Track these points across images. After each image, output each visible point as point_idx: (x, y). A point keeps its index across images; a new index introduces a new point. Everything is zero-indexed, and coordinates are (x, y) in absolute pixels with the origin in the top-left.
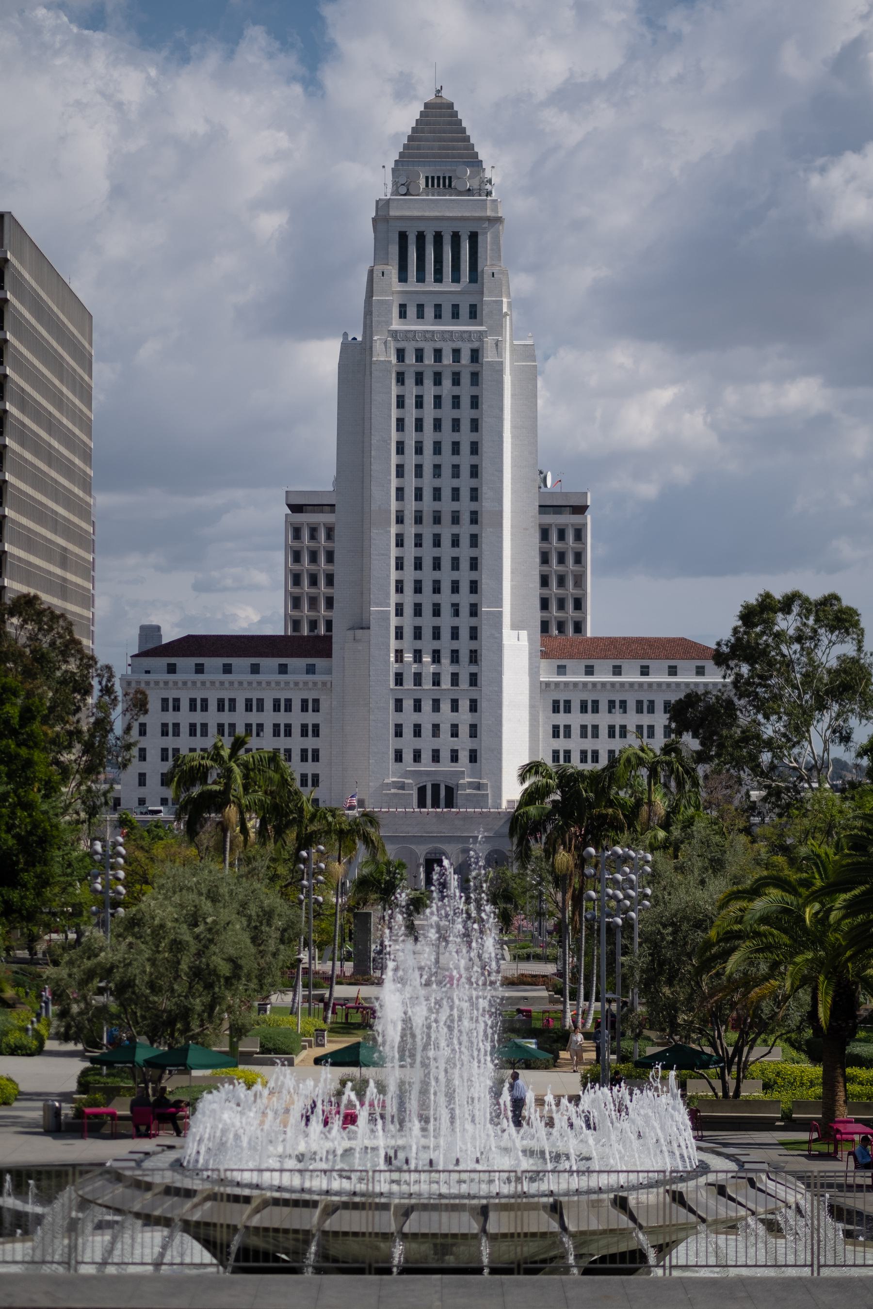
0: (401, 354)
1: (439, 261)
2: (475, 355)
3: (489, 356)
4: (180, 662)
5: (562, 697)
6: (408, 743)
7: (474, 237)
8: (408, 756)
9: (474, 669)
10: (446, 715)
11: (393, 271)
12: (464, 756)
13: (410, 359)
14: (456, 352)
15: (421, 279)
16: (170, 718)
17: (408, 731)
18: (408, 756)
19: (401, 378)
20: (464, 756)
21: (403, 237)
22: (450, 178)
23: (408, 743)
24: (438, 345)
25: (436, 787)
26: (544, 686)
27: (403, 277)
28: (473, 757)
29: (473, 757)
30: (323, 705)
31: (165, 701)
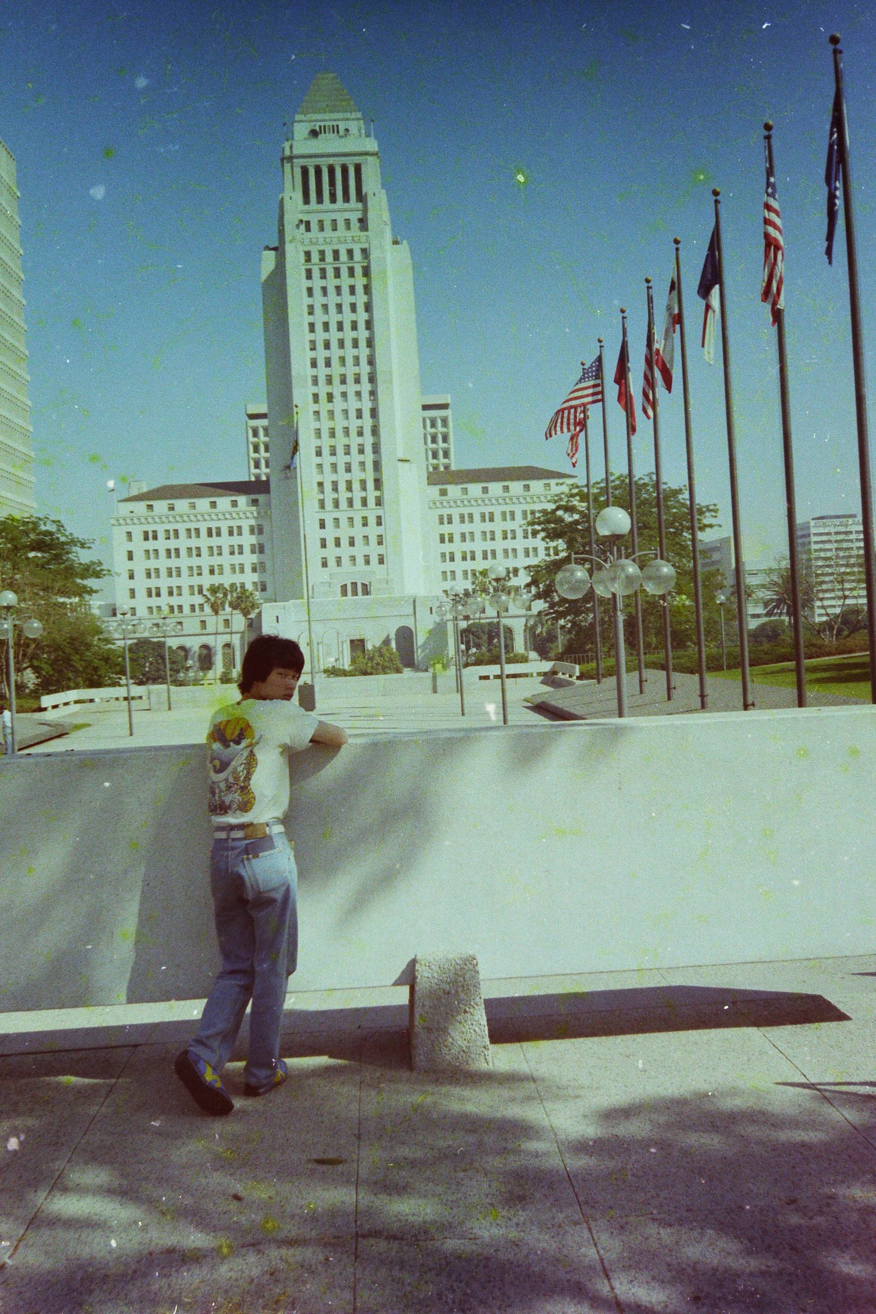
0: (308, 254)
1: (332, 183)
2: (365, 252)
3: (374, 255)
4: (156, 504)
5: (445, 512)
6: (331, 552)
7: (358, 168)
8: (332, 562)
9: (378, 493)
10: (358, 531)
11: (299, 195)
12: (374, 560)
13: (315, 258)
14: (350, 252)
15: (320, 200)
16: (151, 545)
17: (330, 543)
18: (332, 562)
19: (309, 275)
20: (374, 560)
21: (305, 171)
22: (338, 126)
23: (331, 552)
24: (336, 247)
25: (354, 584)
26: (431, 504)
27: (306, 200)
28: (381, 561)
29: (381, 561)
30: (266, 530)
31: (146, 534)
